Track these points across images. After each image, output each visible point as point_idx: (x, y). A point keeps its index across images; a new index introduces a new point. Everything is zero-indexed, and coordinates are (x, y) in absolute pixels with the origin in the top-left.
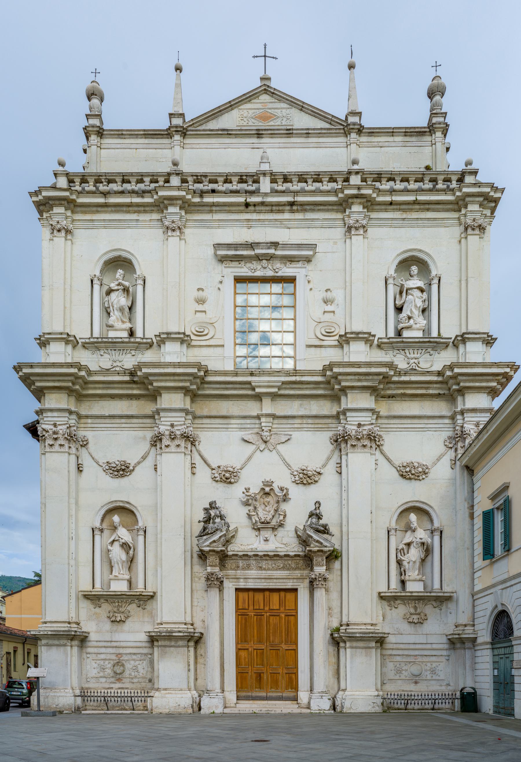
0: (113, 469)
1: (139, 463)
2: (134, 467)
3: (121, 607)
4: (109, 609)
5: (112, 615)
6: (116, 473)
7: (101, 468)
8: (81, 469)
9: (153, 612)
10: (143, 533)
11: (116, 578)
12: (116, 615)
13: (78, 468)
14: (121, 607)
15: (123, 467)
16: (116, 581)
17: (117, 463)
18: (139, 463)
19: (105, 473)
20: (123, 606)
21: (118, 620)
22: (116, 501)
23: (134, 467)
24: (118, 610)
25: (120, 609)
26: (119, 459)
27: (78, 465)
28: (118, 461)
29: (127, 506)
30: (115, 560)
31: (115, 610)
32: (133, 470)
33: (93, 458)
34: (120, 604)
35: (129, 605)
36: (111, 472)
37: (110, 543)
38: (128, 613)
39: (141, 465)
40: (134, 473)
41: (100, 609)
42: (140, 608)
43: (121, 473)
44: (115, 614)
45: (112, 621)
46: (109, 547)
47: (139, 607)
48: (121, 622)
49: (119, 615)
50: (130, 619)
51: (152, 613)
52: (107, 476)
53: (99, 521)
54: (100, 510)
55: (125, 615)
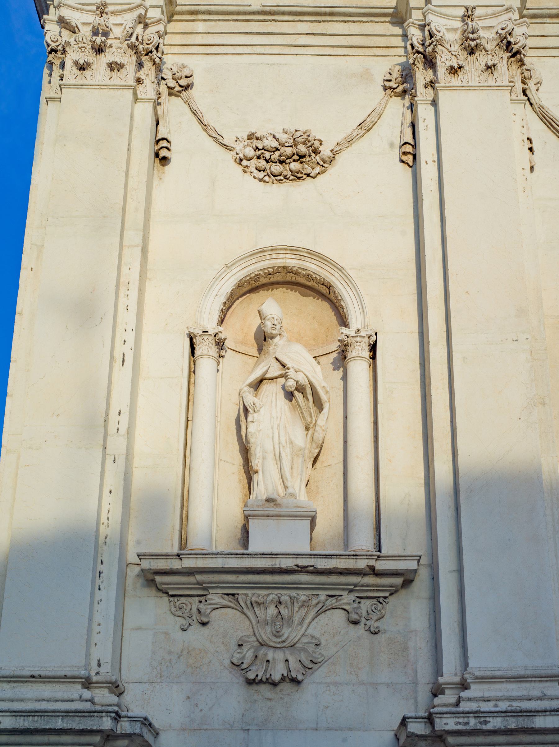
0: (267, 155)
1: (350, 141)
2: (335, 153)
3: (290, 621)
4: (240, 634)
5: (250, 655)
6: (277, 168)
7: (229, 156)
8: (163, 153)
9: (411, 644)
10: (366, 354)
11: (271, 509)
12: (270, 655)
13: (157, 155)
14: (290, 621)
15: (302, 149)
16: (271, 523)
17: (283, 137)
18: (350, 141)
19: (240, 169)
20: (296, 619)
21: (277, 677)
22: (273, 249)
23: (335, 153)
24: (277, 634)
25: (286, 632)
26: (287, 127)
27: (157, 142)
28: (285, 132)
29: (312, 266)
30: (269, 446)
31: (266, 634)
32: (332, 160)
33: (204, 126)
34: (285, 612)
35: (318, 614)
36: (262, 163)
37: (250, 385)
38: (311, 648)
39: (356, 146)
40: (333, 171)
41: (205, 631)
42: (360, 630)
43: (295, 166)
44: (263, 651)
45: (250, 682)
46: (250, 398)
47: (356, 623)
48: (287, 687)
49: (280, 656)
50: (320, 674)
51: (405, 648)
52: (247, 176)
53: (216, 316)
54: (218, 277)
55: (303, 657)
